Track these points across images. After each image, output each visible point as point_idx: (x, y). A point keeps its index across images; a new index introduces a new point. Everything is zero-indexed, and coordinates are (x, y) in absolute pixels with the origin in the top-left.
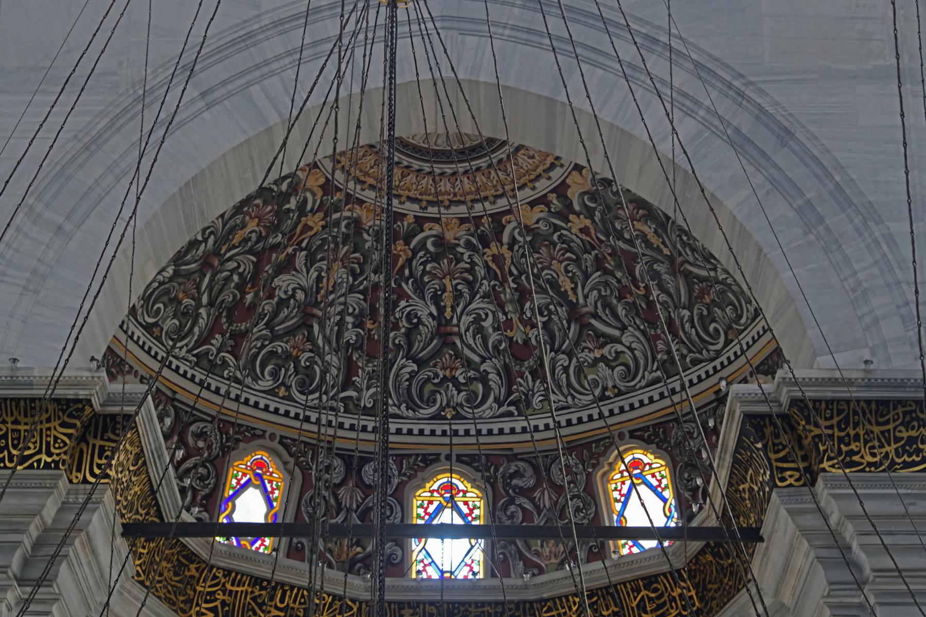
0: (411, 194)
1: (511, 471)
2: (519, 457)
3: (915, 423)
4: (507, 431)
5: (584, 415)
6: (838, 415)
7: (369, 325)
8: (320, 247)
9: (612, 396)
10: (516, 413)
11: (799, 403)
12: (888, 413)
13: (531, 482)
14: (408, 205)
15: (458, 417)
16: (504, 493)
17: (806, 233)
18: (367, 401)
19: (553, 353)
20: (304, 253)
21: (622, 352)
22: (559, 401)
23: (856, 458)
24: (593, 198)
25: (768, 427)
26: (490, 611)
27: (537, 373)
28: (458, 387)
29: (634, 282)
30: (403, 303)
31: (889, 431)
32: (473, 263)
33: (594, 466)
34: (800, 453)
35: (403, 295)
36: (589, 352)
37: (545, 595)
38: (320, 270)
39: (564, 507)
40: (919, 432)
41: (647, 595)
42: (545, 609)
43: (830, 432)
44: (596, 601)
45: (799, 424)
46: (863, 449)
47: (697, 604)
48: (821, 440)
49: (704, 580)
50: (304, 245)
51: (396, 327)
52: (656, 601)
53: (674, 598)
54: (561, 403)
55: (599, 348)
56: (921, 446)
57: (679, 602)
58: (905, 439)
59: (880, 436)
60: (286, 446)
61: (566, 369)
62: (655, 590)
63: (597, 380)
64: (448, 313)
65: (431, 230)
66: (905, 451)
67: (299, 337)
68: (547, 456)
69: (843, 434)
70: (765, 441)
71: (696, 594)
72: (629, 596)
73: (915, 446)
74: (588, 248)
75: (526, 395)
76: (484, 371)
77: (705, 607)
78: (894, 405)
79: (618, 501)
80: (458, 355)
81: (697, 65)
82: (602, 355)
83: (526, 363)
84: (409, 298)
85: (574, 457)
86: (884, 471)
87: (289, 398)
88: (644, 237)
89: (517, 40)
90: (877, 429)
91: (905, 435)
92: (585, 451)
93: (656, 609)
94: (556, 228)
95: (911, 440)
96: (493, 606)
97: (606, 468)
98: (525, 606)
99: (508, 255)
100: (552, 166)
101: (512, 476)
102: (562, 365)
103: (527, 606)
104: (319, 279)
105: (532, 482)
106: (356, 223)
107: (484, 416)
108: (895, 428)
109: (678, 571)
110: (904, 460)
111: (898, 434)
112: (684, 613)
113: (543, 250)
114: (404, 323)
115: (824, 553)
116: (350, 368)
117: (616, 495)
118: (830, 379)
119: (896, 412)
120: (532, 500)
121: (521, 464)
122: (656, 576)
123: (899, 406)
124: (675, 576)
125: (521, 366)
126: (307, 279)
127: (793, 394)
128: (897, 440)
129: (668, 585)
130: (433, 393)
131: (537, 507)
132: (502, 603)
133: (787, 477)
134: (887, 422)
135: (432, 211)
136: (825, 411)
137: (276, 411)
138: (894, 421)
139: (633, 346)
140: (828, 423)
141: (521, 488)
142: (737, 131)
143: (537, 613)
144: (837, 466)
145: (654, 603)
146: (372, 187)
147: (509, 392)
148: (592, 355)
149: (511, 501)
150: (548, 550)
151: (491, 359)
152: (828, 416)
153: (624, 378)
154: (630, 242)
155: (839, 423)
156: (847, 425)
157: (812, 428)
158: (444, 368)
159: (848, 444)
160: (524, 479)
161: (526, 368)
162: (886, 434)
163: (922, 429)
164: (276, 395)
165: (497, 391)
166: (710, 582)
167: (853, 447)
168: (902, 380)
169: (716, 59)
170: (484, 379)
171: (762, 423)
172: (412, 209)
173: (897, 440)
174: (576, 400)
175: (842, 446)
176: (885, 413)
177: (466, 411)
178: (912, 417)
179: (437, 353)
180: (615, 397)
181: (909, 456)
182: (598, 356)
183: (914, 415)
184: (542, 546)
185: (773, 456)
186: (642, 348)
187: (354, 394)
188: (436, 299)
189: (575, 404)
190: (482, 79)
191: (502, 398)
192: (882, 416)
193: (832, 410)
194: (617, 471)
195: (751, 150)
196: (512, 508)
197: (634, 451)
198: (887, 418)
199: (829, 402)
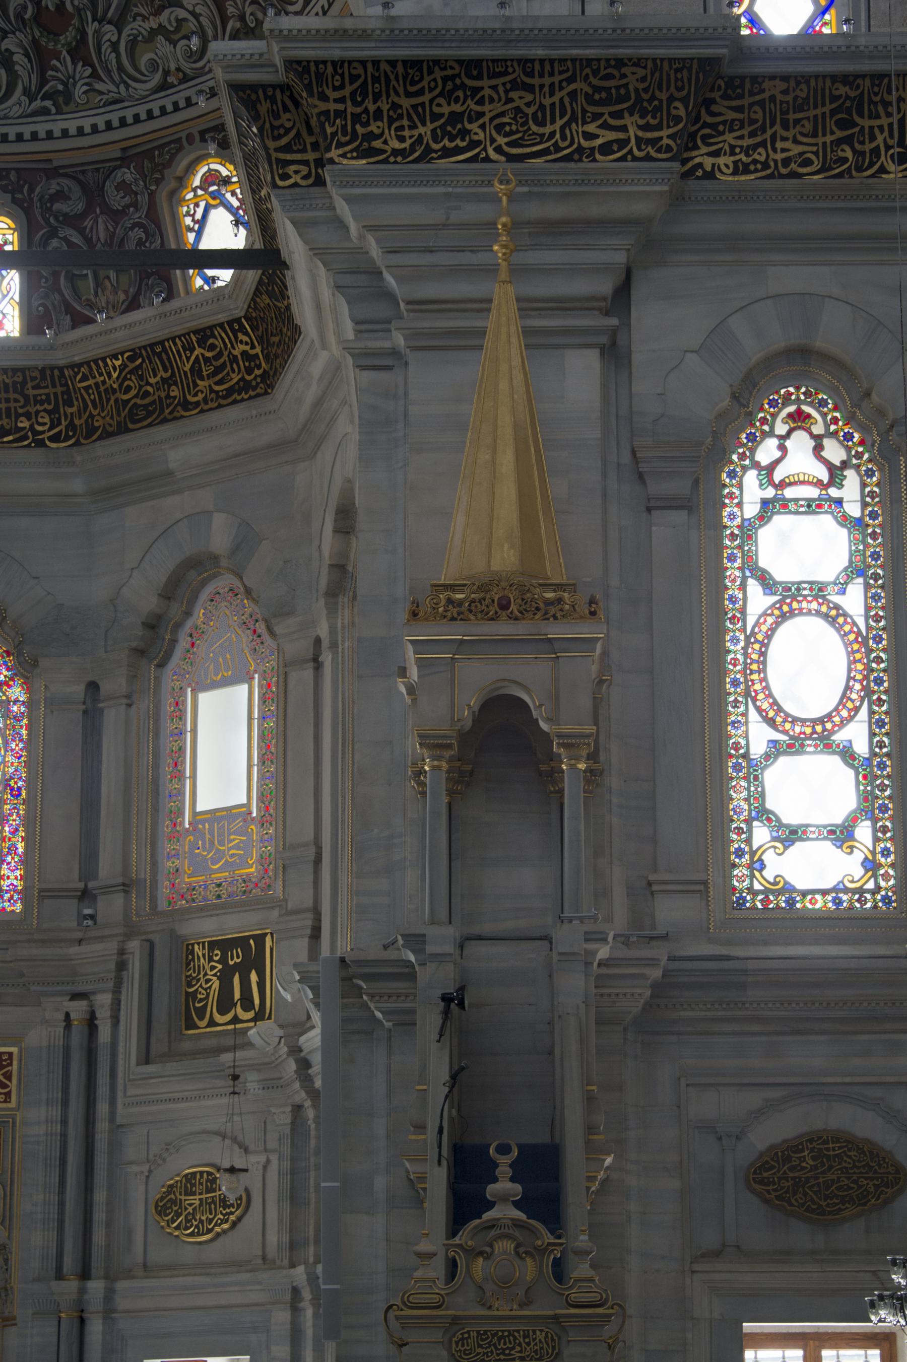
1: (52, 191)
2: (61, 171)
3: (460, 93)
4: (42, 135)
5: (142, 110)
6: (351, 83)
9: (176, 82)
10: (54, 110)
11: (295, 66)
12: (422, 79)
13: (79, 207)
16: (42, 222)
19: (96, 23)
21: (185, 20)
22: (109, 91)
23: (377, 144)
25: (263, 102)
26: (7, 381)
27: (78, 52)
31: (423, 104)
33: (158, 182)
34: (309, 140)
36: (143, 21)
37: (77, 359)
39: (123, 239)
40: (466, 106)
41: (203, 355)
42: (78, 378)
43: (340, 107)
44: (141, 363)
45: (301, 97)
46: (386, 131)
47: (263, 364)
48: (328, 119)
49: (266, 330)
52: (214, 363)
53: (235, 357)
54: (111, 94)
55: (155, 15)
56: (468, 126)
57: (241, 363)
58: (446, 116)
59: (411, 111)
61: (115, 46)
62: (212, 347)
63: (155, 61)
66: (445, 133)
68: (98, 170)
69: (358, 110)
70: (261, 122)
71: (262, 352)
72: (180, 357)
73: (459, 126)
75: (65, 85)
76: (7, 50)
77: (271, 368)
78: (429, 67)
79: (191, 230)
82: (160, 25)
83: (61, 38)
85: (132, 170)
86: (416, 161)
90: (406, 103)
91: (446, 110)
92: (146, 162)
93: (214, 374)
95: (455, 118)
96: (10, 374)
97: (173, 184)
98: (53, 373)
102: (109, 40)
103: (56, 372)
105: (80, 207)
107: (11, 114)
108: (431, 101)
109: (238, 320)
110: (444, 146)
111: (436, 110)
112: (248, 378)
117: (188, 221)
118: (336, 31)
119: (432, 77)
120: (81, 232)
121: (65, 182)
122: (211, 328)
123: (437, 68)
124: (235, 327)
125: (56, 44)
127: (285, 53)
128: (435, 117)
129: (227, 341)
132: (23, 370)
133: (291, 173)
134: (421, 92)
136: (333, 77)
138: (431, 90)
139: (198, 10)
140: (337, 95)
141: (65, 215)
143: (70, 382)
144: (349, 155)
145: (211, 365)
147: (43, 81)
148: (146, 25)
149: (53, 233)
150: (103, 300)
151: (14, 34)
152: (337, 84)
153: (189, 57)
155: (353, 94)
156: (365, 96)
157: (317, 102)
159: (366, 124)
160: (71, 203)
161: (63, 46)
162: (420, 109)
163: (469, 101)
165: (26, 80)
166: (272, 335)
167: (373, 128)
168: (438, 31)
171: (253, 97)
173: (435, 117)
174: (130, 89)
175: (358, 127)
176: (416, 79)
178: (455, 84)
180: (179, 84)
181: (451, 141)
182: (155, 26)
183: (458, 81)
184: (96, 295)
185: (272, 145)
186: (208, 12)
189: (130, 96)
191: (33, 88)
192: (413, 83)
193: (342, 75)
194: (190, 189)
196: (55, 243)
197: (210, 160)
198: (419, 86)
199: (337, 64)
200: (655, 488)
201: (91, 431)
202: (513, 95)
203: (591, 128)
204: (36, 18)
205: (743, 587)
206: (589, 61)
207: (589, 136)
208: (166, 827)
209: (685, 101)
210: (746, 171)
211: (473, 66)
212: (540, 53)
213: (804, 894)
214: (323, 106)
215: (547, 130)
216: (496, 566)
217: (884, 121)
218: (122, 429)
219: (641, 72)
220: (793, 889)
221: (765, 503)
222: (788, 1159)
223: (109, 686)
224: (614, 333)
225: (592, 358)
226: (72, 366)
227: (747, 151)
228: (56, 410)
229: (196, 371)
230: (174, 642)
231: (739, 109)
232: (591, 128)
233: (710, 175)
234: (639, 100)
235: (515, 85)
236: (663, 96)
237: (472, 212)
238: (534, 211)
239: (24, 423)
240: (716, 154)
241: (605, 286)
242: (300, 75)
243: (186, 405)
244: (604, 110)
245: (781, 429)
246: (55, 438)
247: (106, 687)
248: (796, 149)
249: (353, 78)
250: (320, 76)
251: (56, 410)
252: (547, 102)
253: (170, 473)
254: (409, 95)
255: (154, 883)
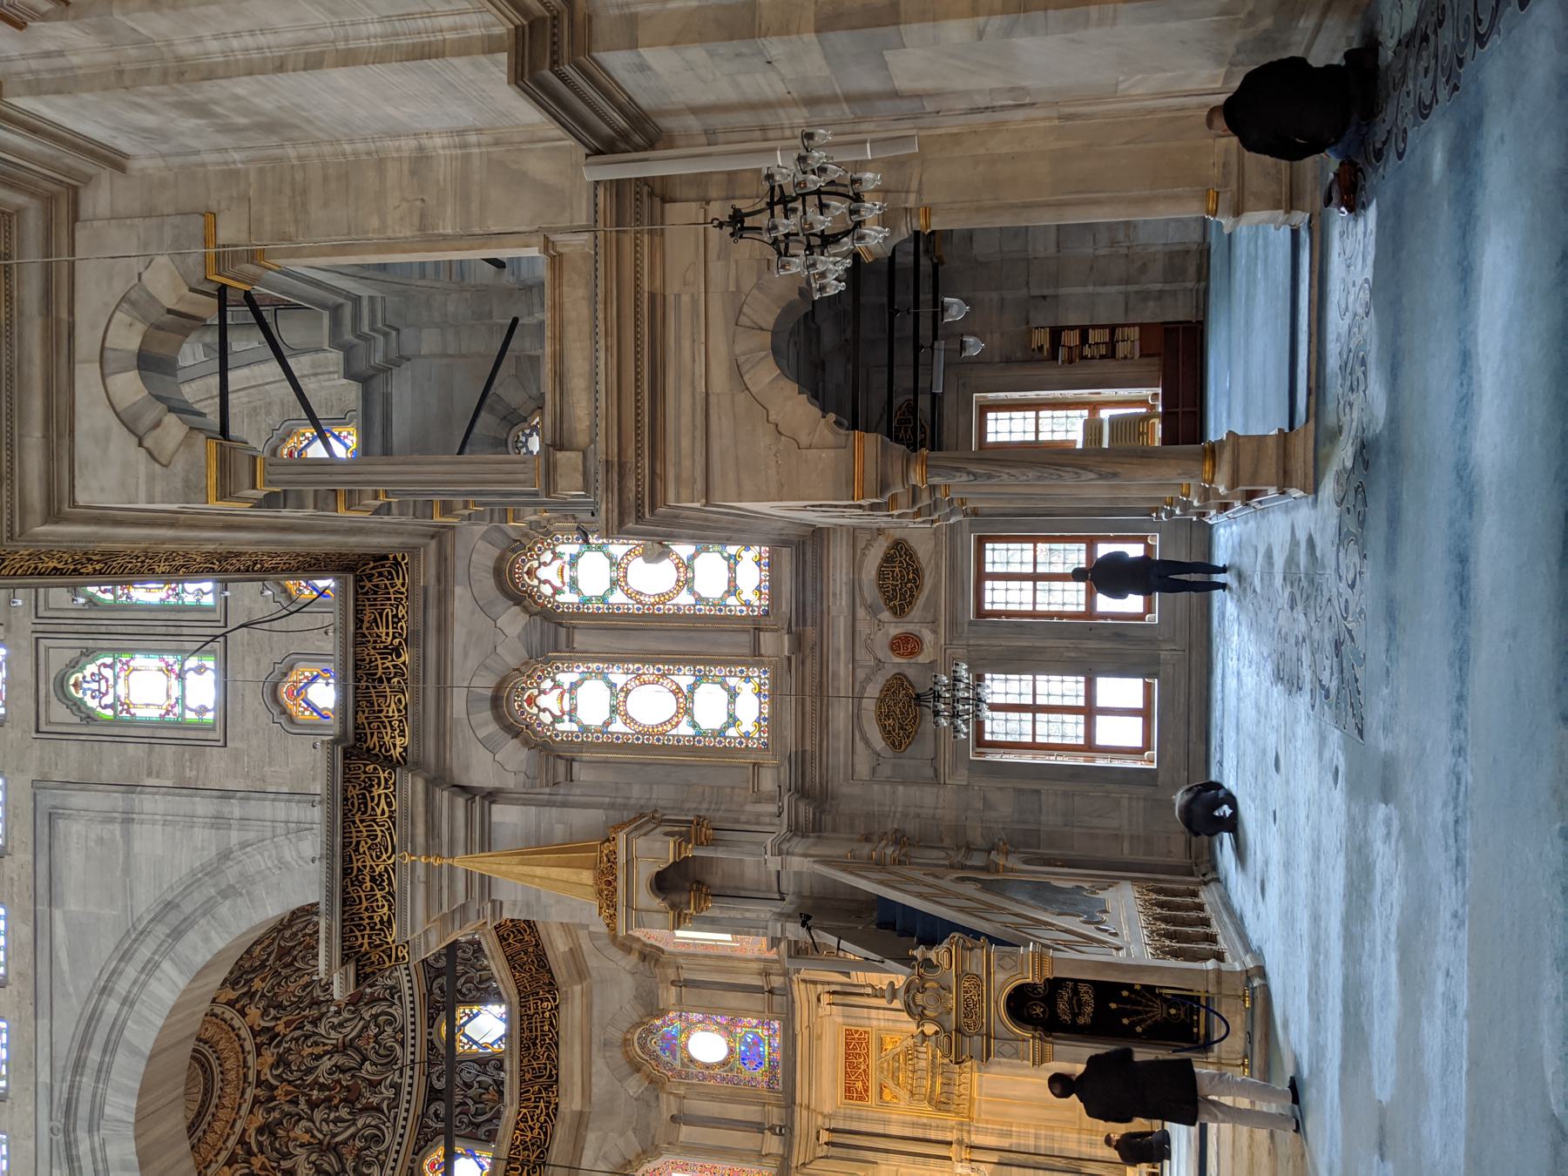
0: (238, 1096)
7: (336, 1101)
8: (277, 1151)
14: (247, 1096)
15: (402, 1030)
17: (241, 895)
18: (391, 1093)
20: (282, 1163)
23: (385, 918)
24: (237, 983)
28: (380, 1033)
29: (300, 944)
30: (321, 1080)
32: (291, 1040)
35: (316, 1082)
38: (296, 1146)
50: (275, 1165)
51: (338, 1081)
60: (420, 1149)
64: (328, 1048)
65: (267, 1075)
66: (380, 884)
67: (344, 1151)
74: (277, 974)
80: (359, 1036)
81: (121, 959)
84: (318, 1076)
87: (387, 1151)
88: (264, 949)
89: (107, 1079)
90: (365, 904)
91: (368, 884)
93: (519, 932)
94: (263, 995)
95: (373, 879)
99: (285, 1019)
100: (216, 1016)
101: (442, 992)
104: (302, 1145)
106: (260, 1131)
113: (280, 999)
114: (335, 1076)
115: (457, 924)
116: (368, 1108)
121: (434, 986)
126: (301, 1154)
128: (372, 889)
130: (385, 1048)
131: (463, 974)
134: (360, 897)
135: (252, 1076)
137: (395, 1161)
142: (168, 936)
146: (232, 1127)
147: (385, 999)
154: (269, 955)
158: (368, 1043)
164: (384, 1162)
167: (377, 920)
169: (117, 947)
170: (375, 1017)
172: (250, 1093)
173: (372, 889)
177: (398, 1025)
179: (358, 1050)
185: (387, 964)
187: (386, 1102)
188: (318, 1057)
190: (135, 1106)
195: (183, 927)
196: (464, 990)
199: (344, 940)
200: (561, 778)
201: (551, 984)
202: (361, 851)
203: (379, 812)
204: (354, 1005)
205: (612, 734)
206: (345, 814)
207: (383, 813)
208: (739, 954)
209: (365, 765)
210: (403, 731)
211: (346, 872)
212: (339, 840)
213: (761, 713)
214: (366, 945)
215: (380, 834)
216: (591, 882)
217: (379, 662)
218: (550, 971)
219: (351, 788)
220: (759, 718)
221: (571, 720)
222: (889, 732)
223: (672, 976)
224: (483, 798)
225: (495, 807)
226: (519, 993)
227: (393, 730)
228: (541, 999)
229: (521, 941)
230: (652, 946)
231: (372, 734)
232: (379, 812)
233: (405, 749)
234: (365, 788)
235: (356, 850)
236: (363, 776)
237: (421, 872)
238: (420, 839)
239: (547, 1015)
240: (395, 746)
241: (460, 802)
242: (349, 958)
243: (537, 945)
244: (370, 805)
245: (535, 710)
246: (555, 1000)
247: (673, 977)
248: (393, 705)
249: (353, 932)
250: (351, 948)
251: (541, 999)
252: (365, 834)
253: (571, 949)
254: (361, 903)
255: (765, 960)
